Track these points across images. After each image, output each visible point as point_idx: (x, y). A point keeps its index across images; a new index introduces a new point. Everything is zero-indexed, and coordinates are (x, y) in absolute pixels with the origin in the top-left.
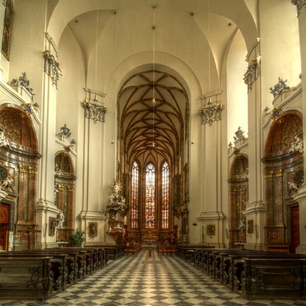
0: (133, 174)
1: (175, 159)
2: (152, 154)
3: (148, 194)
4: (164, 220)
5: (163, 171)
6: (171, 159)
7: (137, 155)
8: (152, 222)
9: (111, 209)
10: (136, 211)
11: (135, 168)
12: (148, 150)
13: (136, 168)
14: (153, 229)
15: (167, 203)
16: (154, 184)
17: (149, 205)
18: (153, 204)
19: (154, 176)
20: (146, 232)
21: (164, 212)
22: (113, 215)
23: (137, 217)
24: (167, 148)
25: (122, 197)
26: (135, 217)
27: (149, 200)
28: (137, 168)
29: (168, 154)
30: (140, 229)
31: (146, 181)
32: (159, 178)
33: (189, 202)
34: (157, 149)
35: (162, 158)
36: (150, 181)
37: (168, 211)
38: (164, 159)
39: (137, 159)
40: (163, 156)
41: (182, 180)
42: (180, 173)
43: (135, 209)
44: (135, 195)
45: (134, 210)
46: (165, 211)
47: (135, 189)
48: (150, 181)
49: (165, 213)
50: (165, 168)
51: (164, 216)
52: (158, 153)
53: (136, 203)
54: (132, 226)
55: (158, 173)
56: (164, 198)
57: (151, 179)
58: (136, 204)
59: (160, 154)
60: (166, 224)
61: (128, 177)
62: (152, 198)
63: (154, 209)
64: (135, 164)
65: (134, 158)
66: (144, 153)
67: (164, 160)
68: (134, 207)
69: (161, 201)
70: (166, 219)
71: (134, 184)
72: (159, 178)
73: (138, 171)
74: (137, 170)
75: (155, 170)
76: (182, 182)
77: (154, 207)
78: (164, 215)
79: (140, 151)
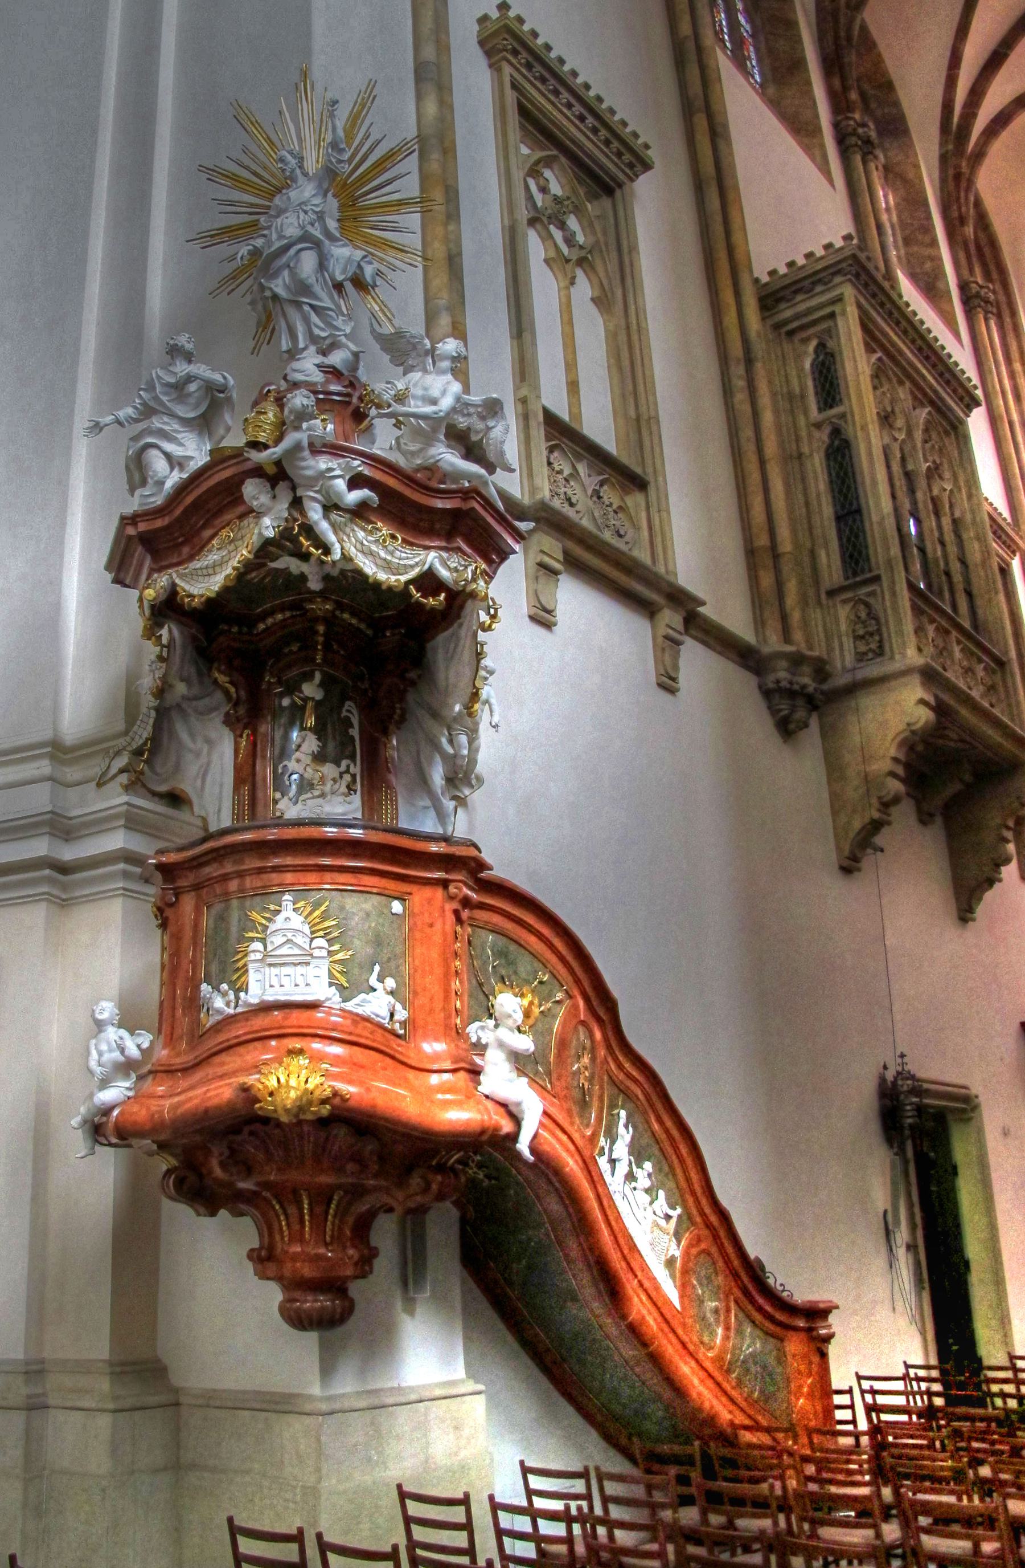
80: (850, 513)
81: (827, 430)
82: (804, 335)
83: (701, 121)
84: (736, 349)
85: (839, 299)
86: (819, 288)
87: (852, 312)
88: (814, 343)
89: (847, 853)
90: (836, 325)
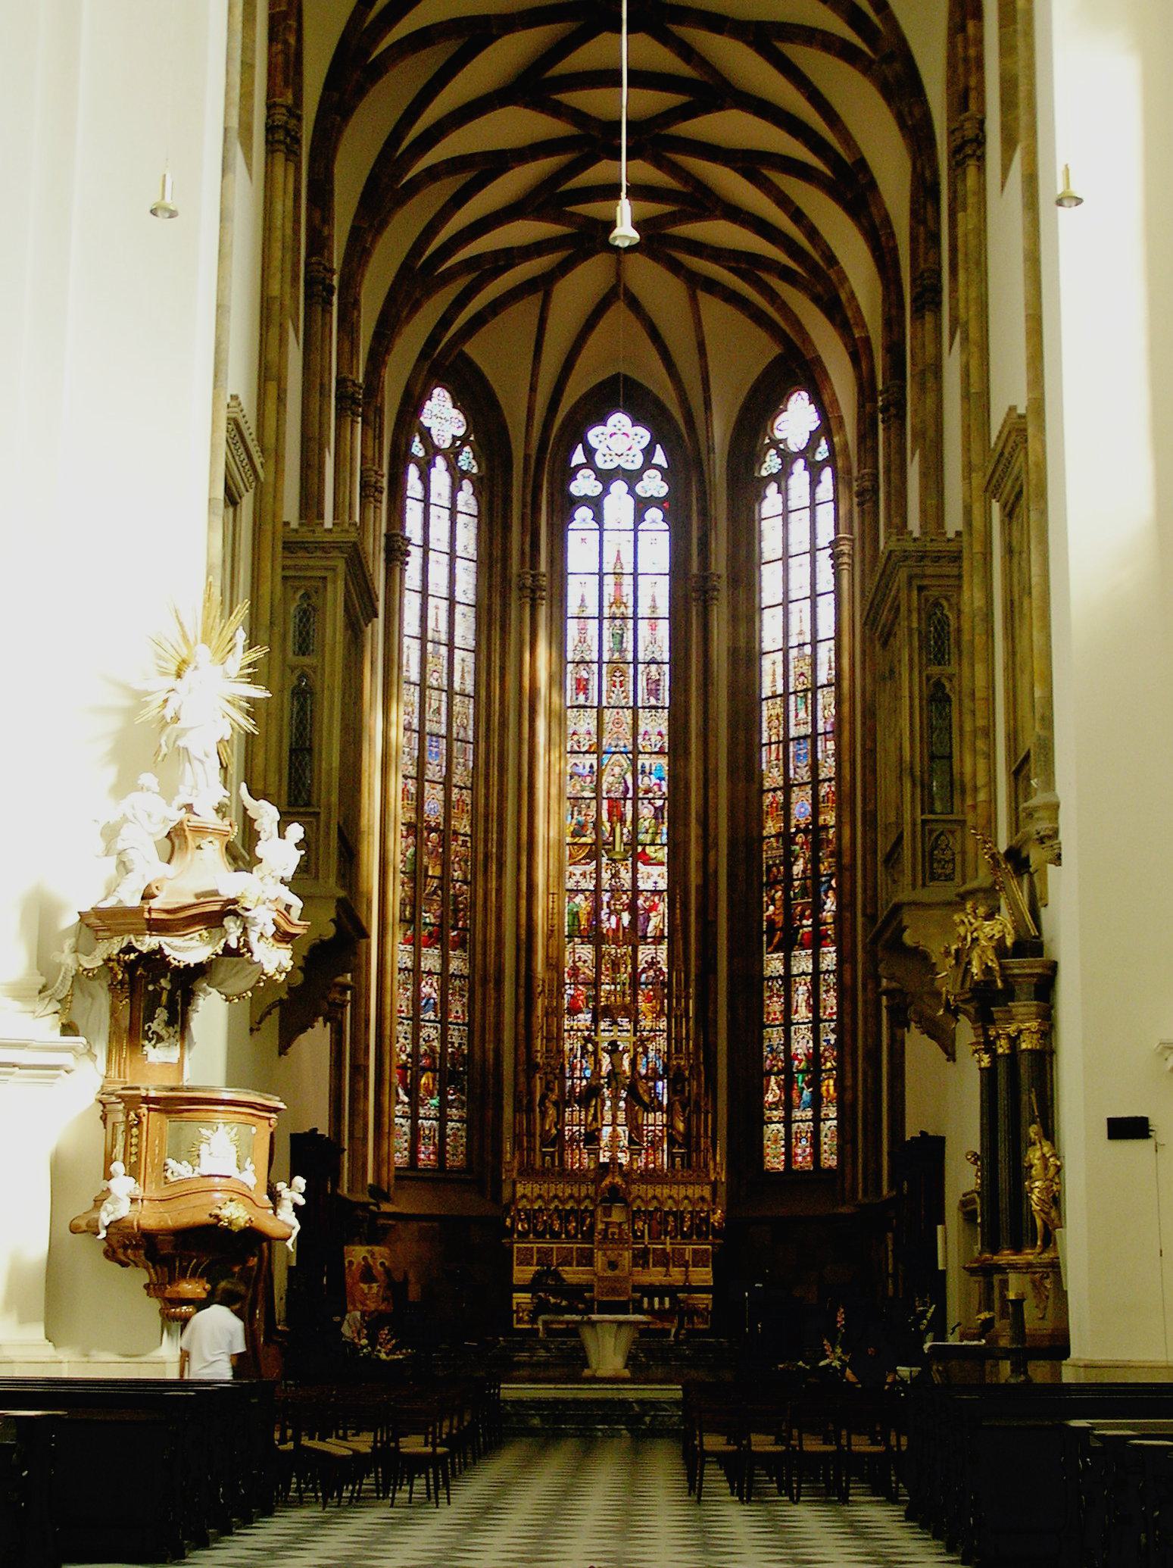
0: (413, 527)
1: (895, 350)
2: (634, 304)
3: (592, 759)
4: (788, 1071)
5: (772, 489)
6: (858, 352)
8: (638, 1100)
9: (130, 949)
10: (445, 961)
11: (440, 461)
12: (587, 255)
13: (452, 455)
14: (650, 1177)
15: (815, 861)
16: (656, 640)
17: (597, 891)
18: (654, 877)
19: (656, 547)
20: (565, 1216)
21: (788, 979)
22: (162, 1014)
23: (455, 1036)
24: (812, 233)
25: (266, 814)
26: (430, 1032)
27: (597, 825)
28: (466, 460)
29: (816, 300)
30: (498, 1184)
31: (572, 609)
32: (720, 564)
33: (1057, 860)
35: (763, 350)
36: (618, 602)
37: (829, 958)
38: (777, 350)
39: (463, 356)
40: (759, 317)
41: (971, 597)
42: (954, 522)
43: (438, 937)
44: (434, 770)
45: (417, 957)
46: (803, 963)
47: (437, 700)
48: (618, 602)
49: (801, 996)
50: (788, 458)
51: (787, 1024)
52: (712, 286)
53: (446, 865)
54: (402, 1143)
55: (704, 513)
56: (787, 806)
57: (628, 580)
58: (445, 879)
59: (732, 298)
60: (817, 1120)
61: (341, 566)
62: (646, 811)
63: (658, 940)
64: (443, 417)
65: (432, 341)
66: (542, 285)
67: (777, 360)
68: (429, 918)
69: (746, 842)
70: (815, 1058)
71: (423, 638)
72: (720, 564)
73: (476, 494)
74: (457, 476)
75: (666, 475)
76: (979, 629)
77: (663, 907)
78: (788, 1010)
79: (497, 272)
80: (302, 750)
81: (298, 672)
82: (297, 584)
83: (272, 387)
84: (265, 619)
85: (334, 569)
86: (319, 554)
87: (341, 584)
88: (301, 592)
89: (258, 1019)
90: (325, 587)
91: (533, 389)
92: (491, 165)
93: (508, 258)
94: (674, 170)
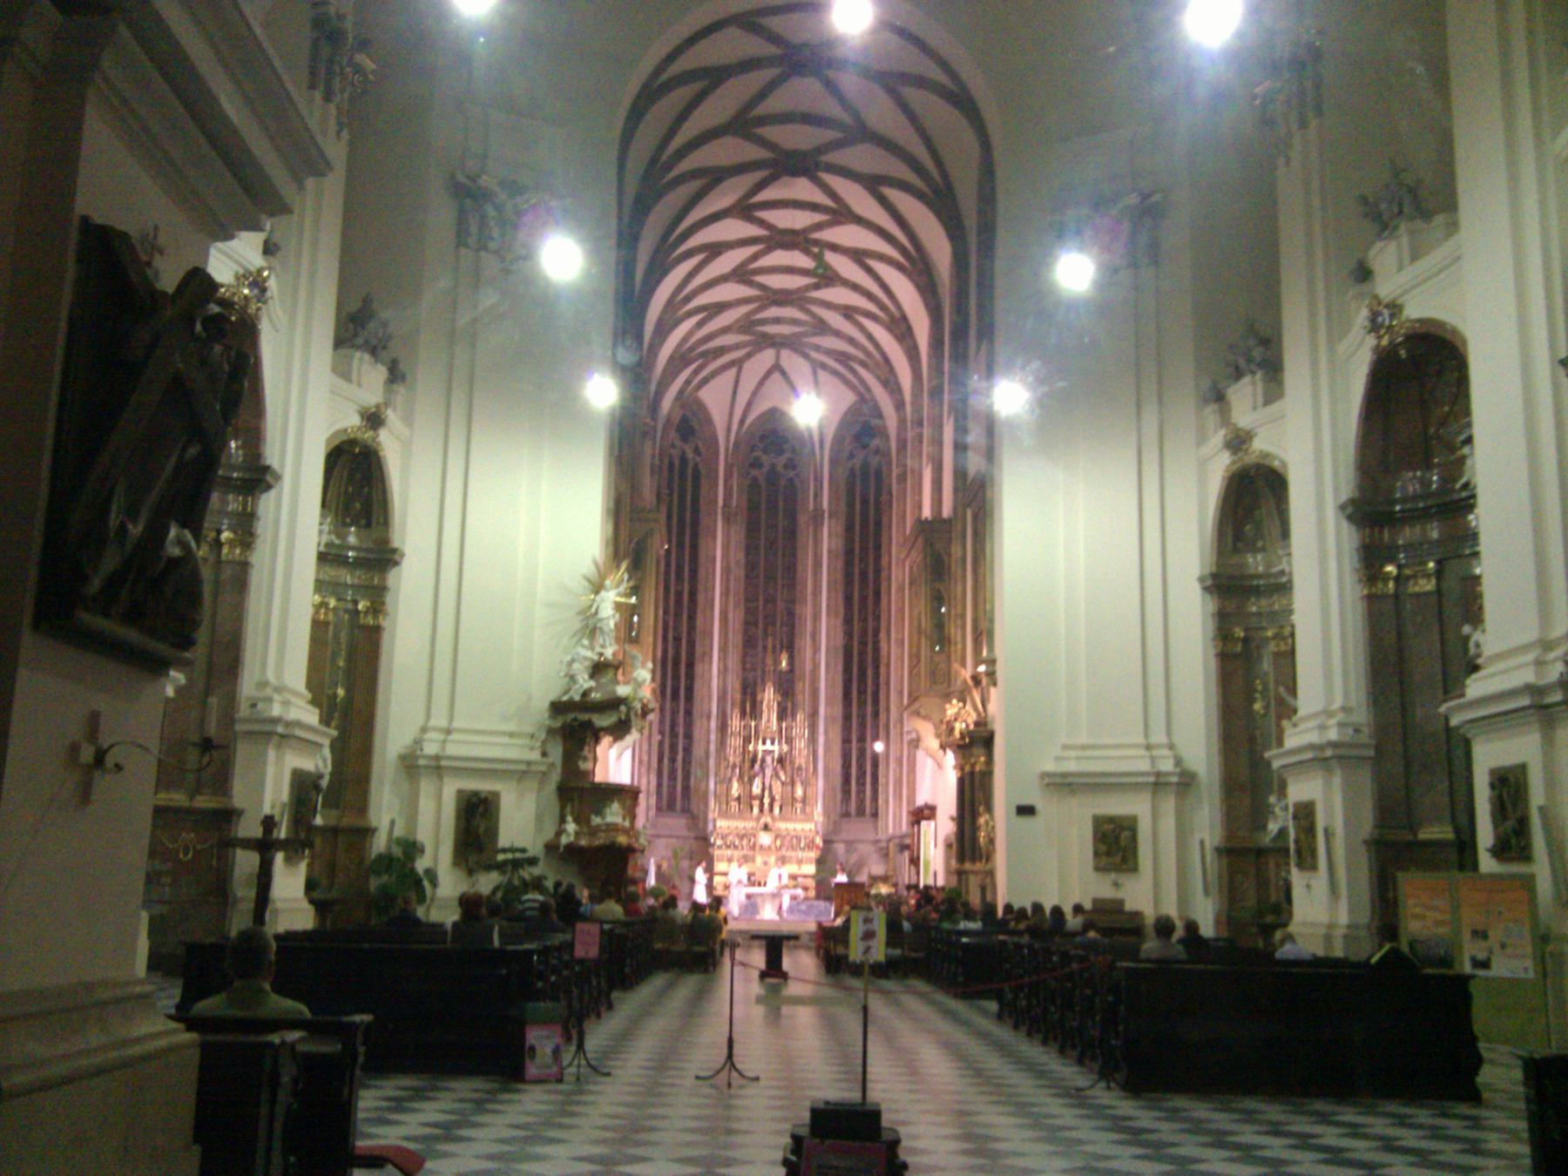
2: (783, 373)
7: (696, 381)
34: (818, 348)
52: (824, 366)
59: (835, 373)
65: (681, 392)
66: (738, 364)
91: (731, 415)
92: (721, 307)
93: (721, 351)
94: (808, 312)
